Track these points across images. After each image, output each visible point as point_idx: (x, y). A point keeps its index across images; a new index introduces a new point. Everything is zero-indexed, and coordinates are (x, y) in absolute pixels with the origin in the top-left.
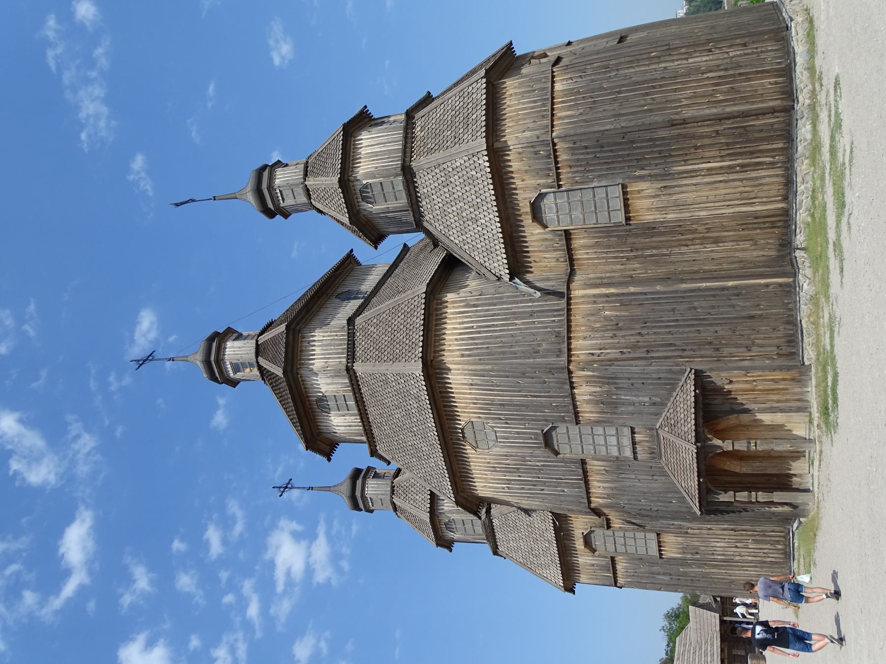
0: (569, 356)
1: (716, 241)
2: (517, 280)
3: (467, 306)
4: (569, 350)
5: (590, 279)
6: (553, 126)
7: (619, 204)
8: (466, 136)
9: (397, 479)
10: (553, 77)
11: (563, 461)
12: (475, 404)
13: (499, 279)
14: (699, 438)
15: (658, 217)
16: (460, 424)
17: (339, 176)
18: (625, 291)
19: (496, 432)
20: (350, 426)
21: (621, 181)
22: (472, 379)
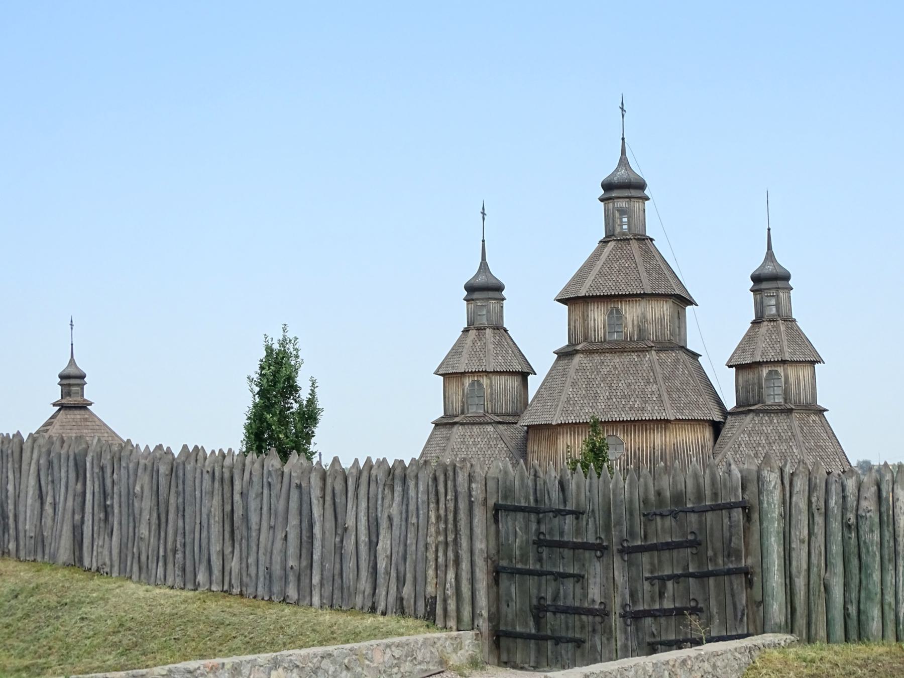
3: (702, 446)
12: (639, 449)
16: (620, 434)
19: (616, 460)
20: (595, 331)
22: (658, 450)
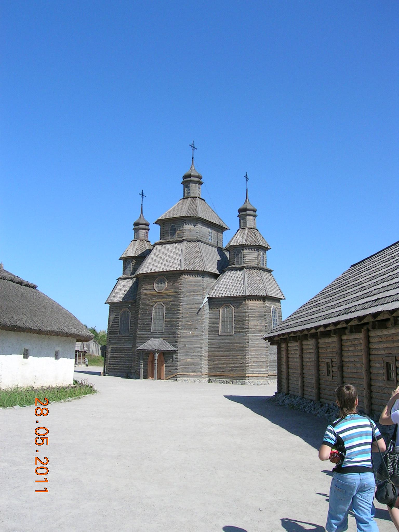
8: (250, 289)
9: (145, 241)
14: (158, 351)
17: (245, 244)
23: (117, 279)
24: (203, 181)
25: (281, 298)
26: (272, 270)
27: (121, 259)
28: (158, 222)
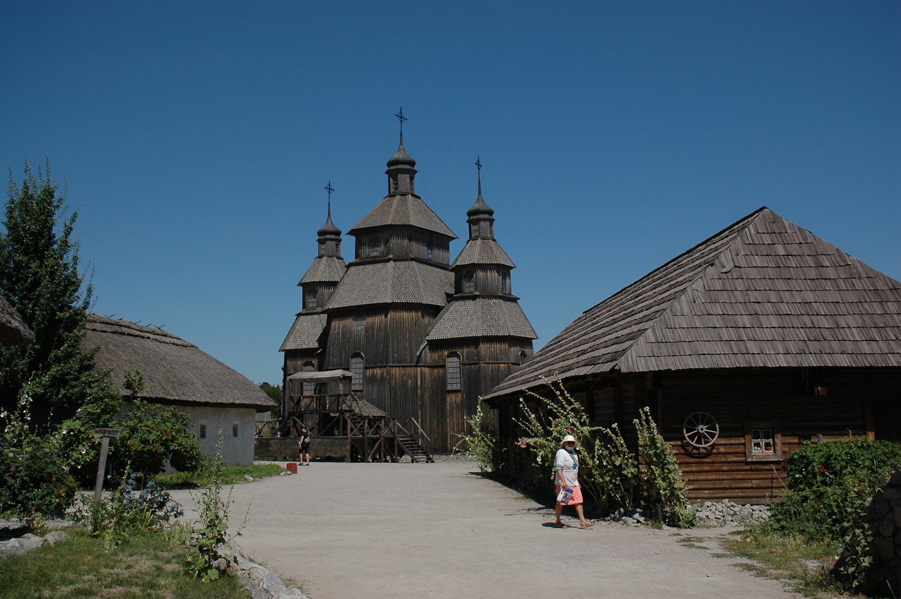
0: (392, 367)
1: (438, 425)
2: (426, 343)
4: (395, 367)
5: (425, 375)
6: (485, 363)
7: (454, 387)
8: (485, 326)
9: (336, 259)
10: (507, 363)
11: (348, 360)
13: (427, 335)
15: (448, 404)
17: (477, 263)
18: (419, 389)
19: (361, 331)
21: (462, 389)
23: (296, 315)
24: (417, 170)
25: (532, 337)
26: (519, 297)
27: (301, 284)
28: (352, 232)
